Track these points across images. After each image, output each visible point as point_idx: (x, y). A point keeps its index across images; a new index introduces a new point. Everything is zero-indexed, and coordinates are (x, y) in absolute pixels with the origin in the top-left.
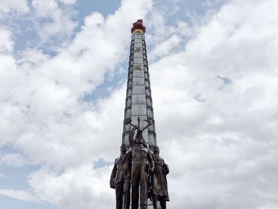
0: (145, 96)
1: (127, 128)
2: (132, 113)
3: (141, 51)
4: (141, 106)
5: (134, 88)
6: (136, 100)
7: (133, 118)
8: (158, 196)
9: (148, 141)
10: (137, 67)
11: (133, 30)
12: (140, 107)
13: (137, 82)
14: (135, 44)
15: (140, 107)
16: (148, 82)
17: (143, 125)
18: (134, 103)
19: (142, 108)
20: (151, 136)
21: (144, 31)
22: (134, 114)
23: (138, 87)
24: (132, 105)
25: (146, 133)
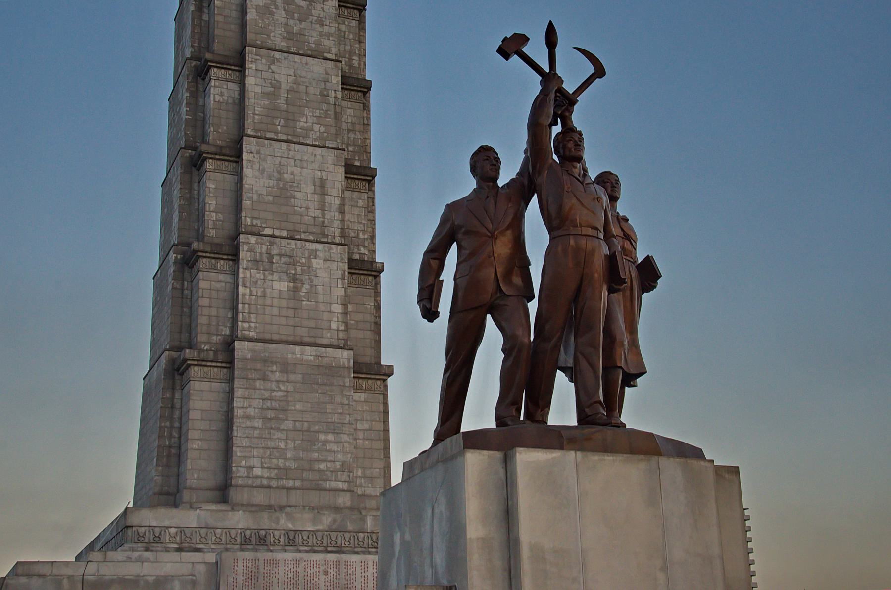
8: (624, 372)
9: (334, 50)
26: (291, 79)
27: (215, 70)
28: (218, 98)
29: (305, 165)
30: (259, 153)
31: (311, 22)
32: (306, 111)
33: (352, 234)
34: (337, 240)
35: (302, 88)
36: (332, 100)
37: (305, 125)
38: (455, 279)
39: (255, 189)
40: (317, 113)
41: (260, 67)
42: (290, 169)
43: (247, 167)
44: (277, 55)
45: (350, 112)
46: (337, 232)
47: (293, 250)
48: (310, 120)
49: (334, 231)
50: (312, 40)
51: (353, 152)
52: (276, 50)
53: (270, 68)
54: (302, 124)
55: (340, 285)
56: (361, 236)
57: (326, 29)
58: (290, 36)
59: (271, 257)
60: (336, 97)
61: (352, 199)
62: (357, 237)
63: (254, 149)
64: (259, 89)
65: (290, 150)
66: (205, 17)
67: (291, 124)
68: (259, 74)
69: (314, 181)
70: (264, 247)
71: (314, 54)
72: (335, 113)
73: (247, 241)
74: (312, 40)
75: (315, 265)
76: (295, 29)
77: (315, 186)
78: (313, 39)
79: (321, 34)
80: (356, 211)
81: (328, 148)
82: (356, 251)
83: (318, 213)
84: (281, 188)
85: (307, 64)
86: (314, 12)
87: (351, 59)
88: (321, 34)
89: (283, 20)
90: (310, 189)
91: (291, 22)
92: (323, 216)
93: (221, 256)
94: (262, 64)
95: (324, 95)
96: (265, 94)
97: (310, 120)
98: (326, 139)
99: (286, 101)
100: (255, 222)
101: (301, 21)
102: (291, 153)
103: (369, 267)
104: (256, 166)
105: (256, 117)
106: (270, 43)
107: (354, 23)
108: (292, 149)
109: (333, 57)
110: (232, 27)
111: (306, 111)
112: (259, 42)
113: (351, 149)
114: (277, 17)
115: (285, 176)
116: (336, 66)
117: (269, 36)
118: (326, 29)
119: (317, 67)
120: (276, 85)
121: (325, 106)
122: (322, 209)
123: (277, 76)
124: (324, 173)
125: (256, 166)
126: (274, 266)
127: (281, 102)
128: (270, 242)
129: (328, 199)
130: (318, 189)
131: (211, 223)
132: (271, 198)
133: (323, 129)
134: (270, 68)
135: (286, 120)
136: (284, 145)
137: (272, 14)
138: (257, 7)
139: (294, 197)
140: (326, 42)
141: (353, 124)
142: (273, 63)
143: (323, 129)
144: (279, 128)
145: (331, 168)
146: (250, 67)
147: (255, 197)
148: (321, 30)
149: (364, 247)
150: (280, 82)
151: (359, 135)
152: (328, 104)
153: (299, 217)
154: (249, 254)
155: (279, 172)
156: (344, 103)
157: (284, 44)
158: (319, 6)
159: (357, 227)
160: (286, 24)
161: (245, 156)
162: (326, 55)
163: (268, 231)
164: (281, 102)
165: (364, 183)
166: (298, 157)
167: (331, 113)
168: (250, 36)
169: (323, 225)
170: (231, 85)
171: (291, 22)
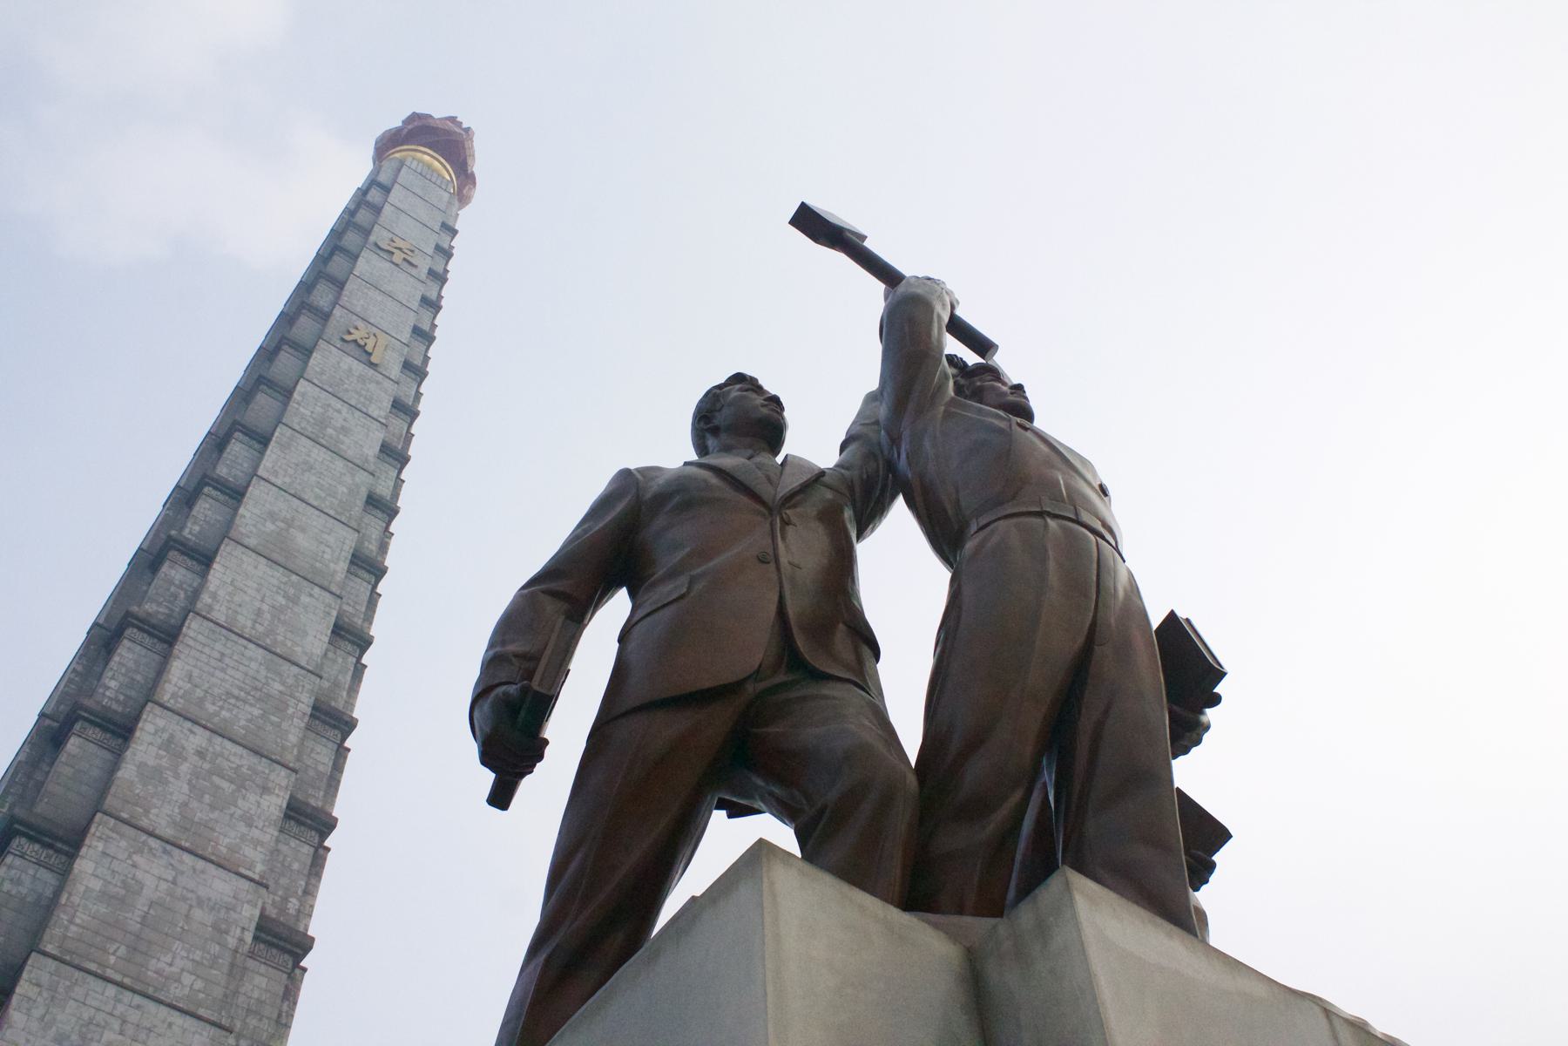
0: (350, 540)
1: (113, 684)
2: (206, 598)
3: (414, 271)
5: (284, 447)
6: (270, 527)
9: (259, 868)
10: (356, 335)
11: (388, 144)
12: (292, 591)
13: (323, 423)
14: (387, 209)
15: (292, 591)
17: (269, 728)
18: (252, 542)
20: (294, 843)
21: (462, 198)
22: (220, 615)
23: (319, 455)
24: (227, 548)
25: (274, 799)
26: (164, 886)
27: (23, 840)
29: (143, 1036)
30: (53, 988)
31: (232, 815)
35: (182, 907)
36: (232, 942)
37: (168, 969)
38: (623, 638)
40: (198, 955)
41: (112, 850)
43: (18, 1009)
44: (153, 843)
45: (261, 981)
48: (179, 963)
52: (151, 834)
53: (130, 857)
54: (161, 965)
60: (241, 940)
63: (45, 978)
64: (96, 885)
65: (119, 1001)
66: (39, 776)
68: (106, 861)
71: (222, 862)
72: (232, 965)
78: (227, 840)
81: (199, 1018)
85: (203, 872)
86: (240, 802)
87: (285, 899)
88: (243, 838)
89: (182, 798)
91: (194, 804)
94: (119, 847)
95: (220, 930)
96: (104, 896)
97: (179, 963)
98: (199, 1005)
99: (144, 918)
101: (212, 807)
102: (120, 1008)
104: (37, 1013)
105: (73, 928)
106: (144, 823)
107: (307, 850)
108: (126, 1000)
109: (256, 877)
110: (84, 788)
111: (177, 945)
112: (125, 815)
117: (147, 812)
118: (256, 833)
119: (221, 886)
120: (132, 888)
121: (215, 949)
123: (139, 875)
125: (37, 1013)
127: (133, 920)
133: (199, 985)
134: (130, 857)
135: (133, 949)
136: (111, 990)
138: (141, 766)
140: (248, 851)
141: (260, 1002)
142: (140, 851)
143: (199, 985)
144: (112, 959)
146: (94, 846)
150: (141, 885)
151: (265, 1024)
152: (223, 945)
156: (251, 963)
160: (185, 804)
161: (23, 988)
162: (242, 870)
164: (133, 920)
166: (134, 1016)
167: (225, 962)
168: (110, 802)
170: (44, 874)
171: (194, 804)
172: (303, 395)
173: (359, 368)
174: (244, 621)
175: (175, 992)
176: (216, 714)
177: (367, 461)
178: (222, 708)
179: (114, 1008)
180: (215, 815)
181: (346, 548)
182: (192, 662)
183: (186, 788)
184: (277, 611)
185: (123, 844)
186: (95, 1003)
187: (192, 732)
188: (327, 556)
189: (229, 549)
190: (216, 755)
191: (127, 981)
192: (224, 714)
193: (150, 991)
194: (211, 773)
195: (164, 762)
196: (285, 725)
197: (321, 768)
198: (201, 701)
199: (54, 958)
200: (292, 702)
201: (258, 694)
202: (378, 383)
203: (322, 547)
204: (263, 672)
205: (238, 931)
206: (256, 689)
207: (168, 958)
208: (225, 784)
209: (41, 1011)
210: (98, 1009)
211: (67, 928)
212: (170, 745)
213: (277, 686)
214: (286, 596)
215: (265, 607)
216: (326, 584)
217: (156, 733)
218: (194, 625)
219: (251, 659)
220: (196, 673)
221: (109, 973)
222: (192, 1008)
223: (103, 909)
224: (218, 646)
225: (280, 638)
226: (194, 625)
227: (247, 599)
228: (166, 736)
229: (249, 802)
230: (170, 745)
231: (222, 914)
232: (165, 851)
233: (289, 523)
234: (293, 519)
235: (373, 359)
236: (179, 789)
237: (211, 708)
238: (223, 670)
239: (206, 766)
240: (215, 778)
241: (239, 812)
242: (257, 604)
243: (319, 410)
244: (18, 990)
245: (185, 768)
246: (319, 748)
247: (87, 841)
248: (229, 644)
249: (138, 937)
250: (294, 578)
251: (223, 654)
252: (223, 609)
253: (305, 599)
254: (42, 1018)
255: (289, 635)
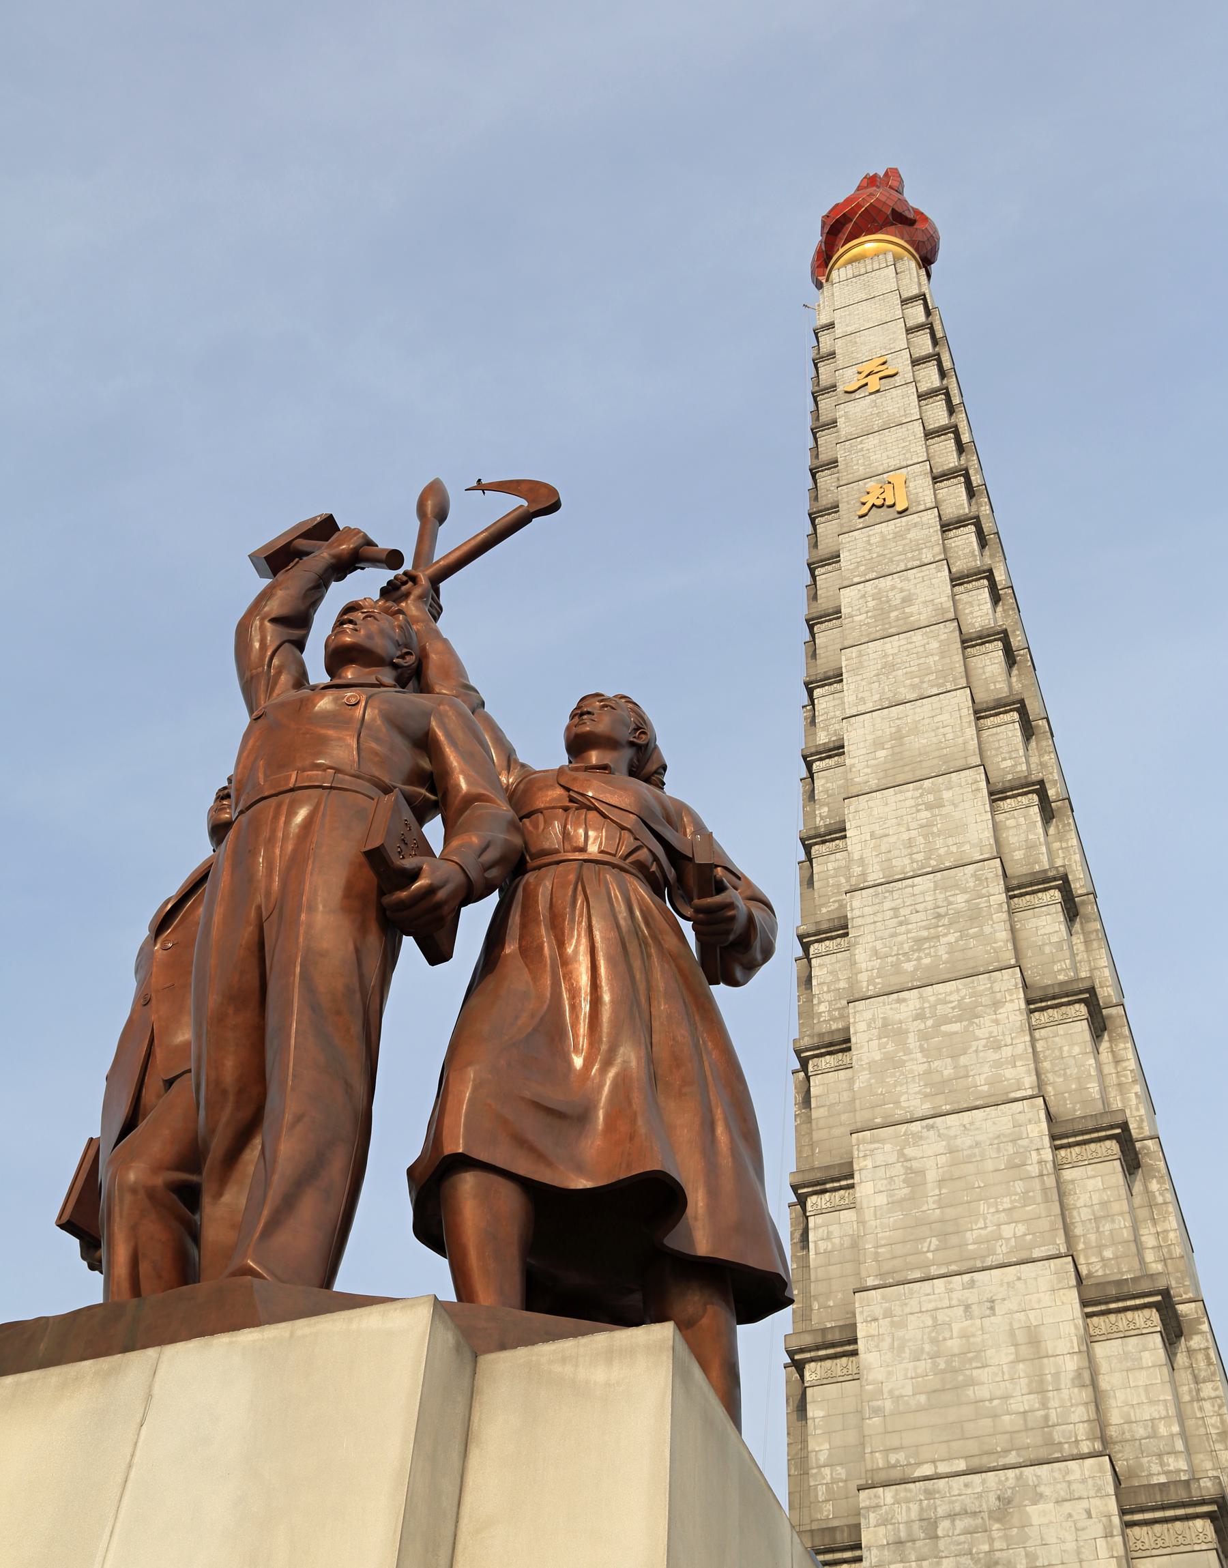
1: (823, 1008)
2: (857, 870)
3: (898, 380)
4: (935, 791)
6: (881, 754)
7: (867, 910)
9: (1029, 1081)
10: (871, 500)
12: (931, 797)
13: (882, 612)
15: (931, 797)
16: (985, 594)
17: (972, 942)
19: (944, 811)
20: (1061, 1029)
28: (822, 1246)
31: (976, 1051)
32: (983, 1207)
33: (1141, 1432)
34: (1085, 1448)
36: (1034, 1170)
39: (885, 1390)
40: (1006, 1203)
41: (880, 1159)
42: (956, 1327)
44: (915, 1127)
46: (1082, 1430)
47: (979, 1496)
49: (1075, 1426)
50: (980, 1080)
51: (1116, 1258)
55: (1103, 1552)
56: (1163, 1430)
57: (1007, 1052)
58: (938, 1087)
59: (930, 1527)
61: (1126, 1355)
62: (1154, 1435)
63: (878, 1311)
64: (882, 1200)
65: (951, 1290)
67: (954, 1240)
68: (881, 1172)
69: (1012, 1333)
70: (914, 1507)
73: (874, 1502)
74: (980, 1080)
75: (1036, 1520)
76: (948, 1072)
77: (1016, 1345)
79: (998, 1064)
80: (1141, 1378)
82: (1156, 1468)
83: (1033, 1401)
84: (944, 1372)
86: (978, 1033)
90: (1002, 1356)
92: (1044, 1405)
93: (838, 1556)
100: (893, 1458)
102: (955, 1295)
103: (1183, 1495)
106: (899, 1114)
109: (1029, 1092)
111: (983, 1207)
112: (878, 1120)
113: (1108, 1253)
114: (909, 1066)
115: (949, 1343)
116: (1033, 1106)
117: (897, 1103)
118: (1007, 1052)
120: (915, 1178)
121: (1019, 1186)
122: (1039, 1388)
123: (915, 1164)
124: (1032, 1314)
125: (886, 1344)
126: (942, 1544)
128: (927, 1491)
129: (1049, 1366)
130: (1025, 1351)
131: (822, 1490)
132: (922, 1399)
133: (1021, 1229)
135: (943, 1236)
137: (899, 1064)
139: (972, 1382)
140: (1009, 1073)
141: (1104, 1204)
143: (1021, 1229)
145: (1047, 1299)
146: (863, 1167)
147: (888, 1405)
148: (997, 1056)
149: (1174, 1453)
153: (988, 1422)
154: (882, 1530)
155: (934, 1341)
157: (927, 1106)
158: (987, 1021)
159: (1147, 1413)
160: (928, 1072)
163: (919, 1473)
165: (1147, 1312)
166: (971, 1296)
169: (1046, 1423)
172: (850, 605)
173: (888, 528)
174: (902, 864)
175: (1001, 1252)
176: (916, 969)
177: (944, 611)
178: (919, 959)
179: (950, 1299)
180: (963, 1060)
181: (965, 712)
182: (870, 938)
183: (919, 1055)
184: (929, 825)
185: (888, 1147)
186: (931, 1306)
187: (899, 1001)
188: (950, 736)
189: (852, 809)
190: (933, 1007)
191: (953, 1268)
192: (927, 961)
193: (979, 1264)
194: (937, 1025)
195: (890, 1047)
196: (987, 929)
197: (1055, 939)
198: (896, 965)
199: (875, 1288)
200: (982, 903)
201: (946, 921)
202: (915, 525)
203: (941, 730)
204: (941, 896)
205: (1034, 1154)
206: (939, 916)
207: (981, 1224)
208: (956, 1027)
209: (888, 1340)
210: (937, 1309)
211: (877, 1253)
212: (889, 1030)
213: (961, 898)
214: (929, 807)
215: (914, 833)
216: (960, 763)
217: (869, 1025)
218: (856, 904)
219: (923, 893)
220: (879, 945)
221: (934, 1271)
222: (1024, 1255)
223: (898, 1215)
224: (887, 905)
225: (942, 851)
226: (856, 904)
227: (892, 839)
228: (879, 1023)
229: (985, 1027)
230: (889, 1030)
231: (1010, 1149)
232: (929, 1128)
233: (898, 737)
234: (899, 729)
235: (899, 508)
236: (916, 1063)
237: (909, 966)
238: (901, 924)
239: (930, 1023)
240: (943, 1028)
241: (983, 1042)
242: (905, 836)
243: (871, 604)
244: (859, 1335)
245: (912, 1041)
246: (1042, 921)
247: (856, 1167)
248: (896, 895)
249: (942, 1221)
250: (927, 783)
251: (894, 909)
252: (877, 867)
253: (947, 795)
254: (892, 1348)
255: (950, 841)
